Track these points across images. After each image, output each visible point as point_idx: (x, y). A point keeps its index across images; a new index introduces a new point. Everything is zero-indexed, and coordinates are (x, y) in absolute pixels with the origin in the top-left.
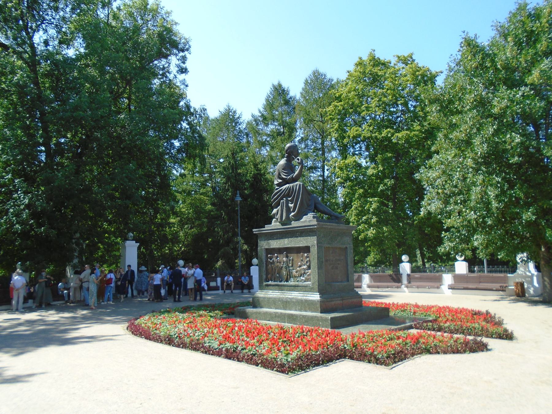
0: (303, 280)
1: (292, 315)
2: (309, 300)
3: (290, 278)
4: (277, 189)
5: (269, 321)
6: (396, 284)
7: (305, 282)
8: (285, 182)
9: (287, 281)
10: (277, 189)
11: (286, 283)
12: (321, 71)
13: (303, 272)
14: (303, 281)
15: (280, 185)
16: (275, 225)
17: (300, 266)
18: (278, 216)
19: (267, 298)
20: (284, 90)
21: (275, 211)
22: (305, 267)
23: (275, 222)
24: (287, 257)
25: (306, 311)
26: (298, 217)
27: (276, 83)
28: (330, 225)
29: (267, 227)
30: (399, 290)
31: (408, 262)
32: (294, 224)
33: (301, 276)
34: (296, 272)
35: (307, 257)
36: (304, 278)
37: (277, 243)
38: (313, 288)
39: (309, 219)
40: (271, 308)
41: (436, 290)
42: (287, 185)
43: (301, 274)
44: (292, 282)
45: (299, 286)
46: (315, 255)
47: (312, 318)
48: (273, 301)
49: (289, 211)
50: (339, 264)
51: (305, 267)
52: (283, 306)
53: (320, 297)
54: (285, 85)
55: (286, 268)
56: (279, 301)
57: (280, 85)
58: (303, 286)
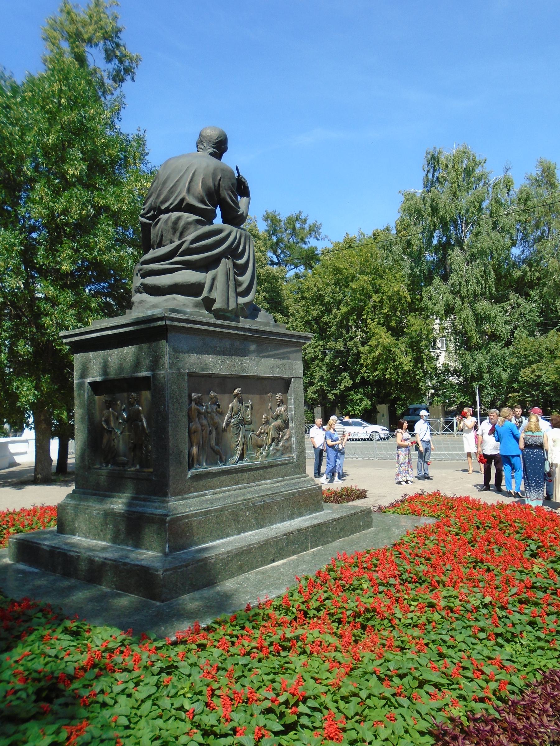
2: (306, 490)
5: (273, 561)
7: (282, 454)
11: (240, 464)
14: (278, 454)
17: (267, 422)
19: (216, 511)
24: (241, 401)
25: (300, 515)
32: (244, 323)
35: (282, 402)
37: (224, 362)
38: (299, 464)
40: (228, 535)
45: (276, 465)
48: (232, 513)
52: (256, 518)
56: (248, 509)
58: (282, 465)
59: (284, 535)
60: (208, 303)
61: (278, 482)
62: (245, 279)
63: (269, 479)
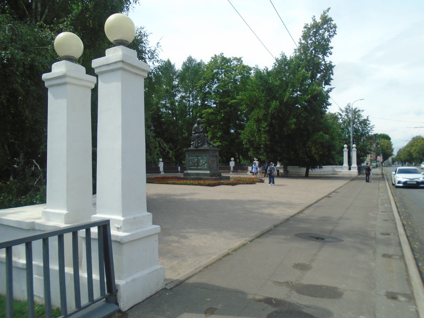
1: (200, 178)
4: (193, 135)
6: (228, 171)
8: (197, 133)
9: (197, 167)
10: (193, 135)
15: (194, 134)
16: (192, 148)
18: (194, 145)
21: (192, 143)
23: (192, 146)
26: (202, 145)
29: (189, 148)
30: (229, 173)
39: (206, 146)
41: (245, 173)
42: (198, 134)
44: (199, 168)
47: (208, 178)
49: (198, 143)
54: (172, 63)
60: (193, 146)
62: (200, 141)
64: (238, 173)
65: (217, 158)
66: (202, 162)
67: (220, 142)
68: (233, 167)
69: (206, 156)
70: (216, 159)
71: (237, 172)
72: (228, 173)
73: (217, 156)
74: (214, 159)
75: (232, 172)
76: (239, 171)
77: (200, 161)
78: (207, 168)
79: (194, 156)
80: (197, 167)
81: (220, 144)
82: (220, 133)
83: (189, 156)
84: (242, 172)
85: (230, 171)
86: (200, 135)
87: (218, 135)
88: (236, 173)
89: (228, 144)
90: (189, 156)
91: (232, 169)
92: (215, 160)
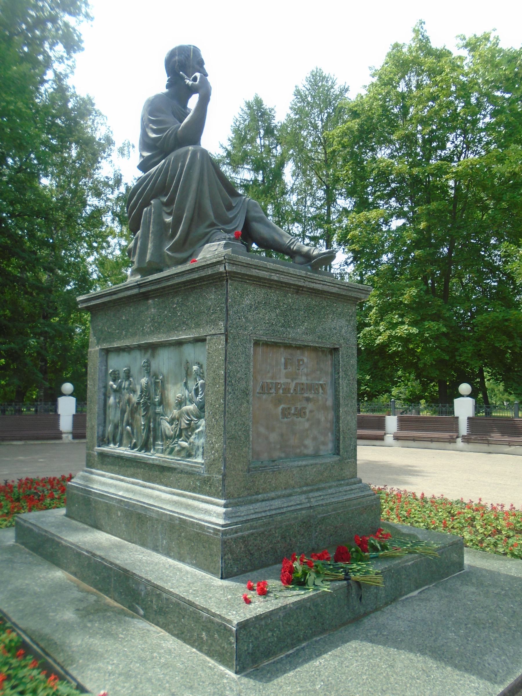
0: (183, 448)
2: (193, 523)
3: (155, 439)
6: (446, 435)
11: (142, 455)
12: (325, 73)
13: (184, 423)
14: (183, 453)
20: (264, 114)
22: (190, 407)
27: (251, 99)
28: (276, 271)
30: (452, 445)
31: (469, 396)
33: (180, 436)
34: (171, 422)
36: (185, 444)
38: (209, 479)
43: (181, 430)
46: (219, 367)
50: (308, 399)
51: (190, 407)
53: (227, 516)
54: (267, 105)
55: (147, 409)
57: (259, 102)
59: (87, 552)
61: (174, 494)
63: (166, 486)
64: (492, 448)
65: (335, 366)
66: (180, 403)
67: (413, 324)
68: (469, 418)
69: (202, 340)
70: (326, 380)
71: (489, 443)
72: (447, 445)
73: (334, 351)
74: (303, 380)
75: (467, 440)
76: (496, 436)
77: (163, 389)
78: (209, 466)
79: (128, 349)
80: (146, 447)
81: (415, 330)
82: (414, 291)
83: (107, 352)
84: (510, 444)
85: (454, 435)
86: (176, 160)
87: (406, 299)
88: (485, 447)
89: (444, 330)
90: (107, 352)
91: (463, 428)
92: (310, 387)
